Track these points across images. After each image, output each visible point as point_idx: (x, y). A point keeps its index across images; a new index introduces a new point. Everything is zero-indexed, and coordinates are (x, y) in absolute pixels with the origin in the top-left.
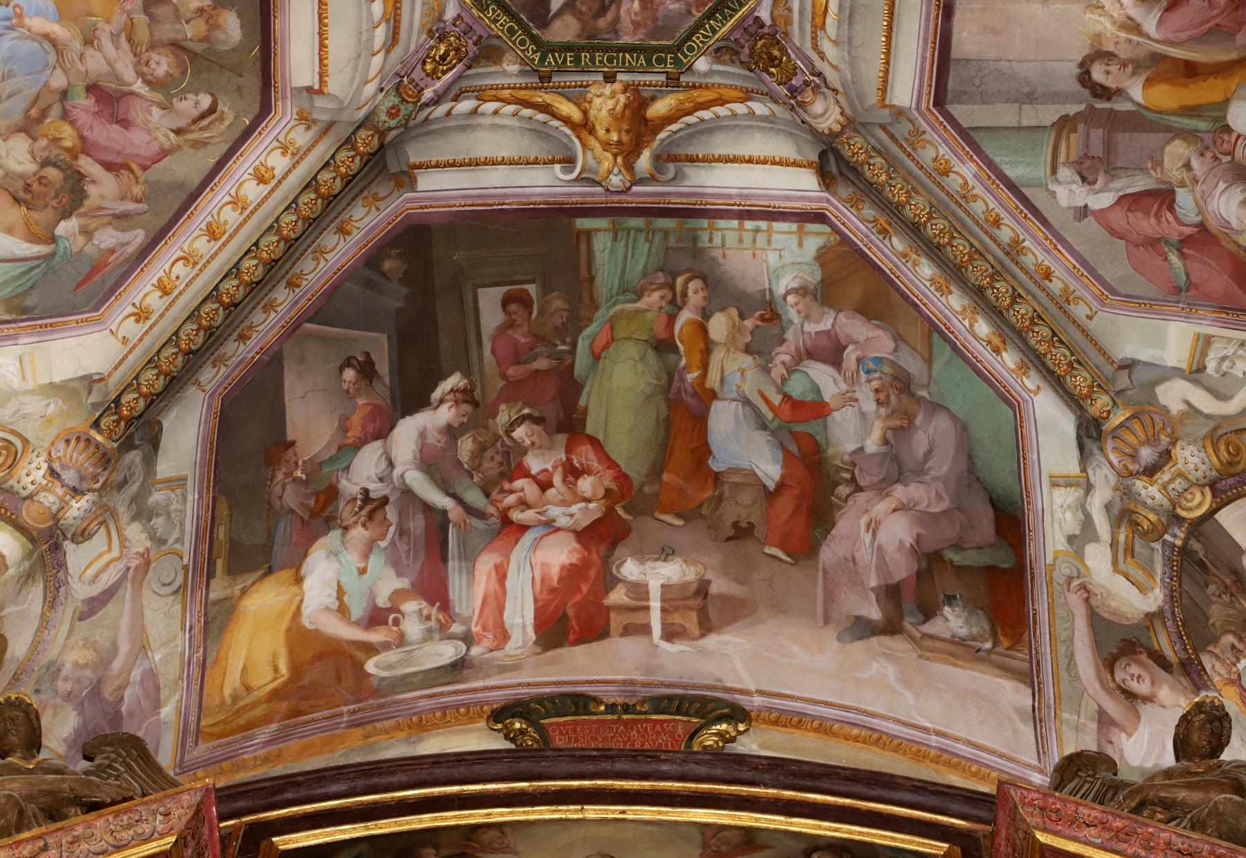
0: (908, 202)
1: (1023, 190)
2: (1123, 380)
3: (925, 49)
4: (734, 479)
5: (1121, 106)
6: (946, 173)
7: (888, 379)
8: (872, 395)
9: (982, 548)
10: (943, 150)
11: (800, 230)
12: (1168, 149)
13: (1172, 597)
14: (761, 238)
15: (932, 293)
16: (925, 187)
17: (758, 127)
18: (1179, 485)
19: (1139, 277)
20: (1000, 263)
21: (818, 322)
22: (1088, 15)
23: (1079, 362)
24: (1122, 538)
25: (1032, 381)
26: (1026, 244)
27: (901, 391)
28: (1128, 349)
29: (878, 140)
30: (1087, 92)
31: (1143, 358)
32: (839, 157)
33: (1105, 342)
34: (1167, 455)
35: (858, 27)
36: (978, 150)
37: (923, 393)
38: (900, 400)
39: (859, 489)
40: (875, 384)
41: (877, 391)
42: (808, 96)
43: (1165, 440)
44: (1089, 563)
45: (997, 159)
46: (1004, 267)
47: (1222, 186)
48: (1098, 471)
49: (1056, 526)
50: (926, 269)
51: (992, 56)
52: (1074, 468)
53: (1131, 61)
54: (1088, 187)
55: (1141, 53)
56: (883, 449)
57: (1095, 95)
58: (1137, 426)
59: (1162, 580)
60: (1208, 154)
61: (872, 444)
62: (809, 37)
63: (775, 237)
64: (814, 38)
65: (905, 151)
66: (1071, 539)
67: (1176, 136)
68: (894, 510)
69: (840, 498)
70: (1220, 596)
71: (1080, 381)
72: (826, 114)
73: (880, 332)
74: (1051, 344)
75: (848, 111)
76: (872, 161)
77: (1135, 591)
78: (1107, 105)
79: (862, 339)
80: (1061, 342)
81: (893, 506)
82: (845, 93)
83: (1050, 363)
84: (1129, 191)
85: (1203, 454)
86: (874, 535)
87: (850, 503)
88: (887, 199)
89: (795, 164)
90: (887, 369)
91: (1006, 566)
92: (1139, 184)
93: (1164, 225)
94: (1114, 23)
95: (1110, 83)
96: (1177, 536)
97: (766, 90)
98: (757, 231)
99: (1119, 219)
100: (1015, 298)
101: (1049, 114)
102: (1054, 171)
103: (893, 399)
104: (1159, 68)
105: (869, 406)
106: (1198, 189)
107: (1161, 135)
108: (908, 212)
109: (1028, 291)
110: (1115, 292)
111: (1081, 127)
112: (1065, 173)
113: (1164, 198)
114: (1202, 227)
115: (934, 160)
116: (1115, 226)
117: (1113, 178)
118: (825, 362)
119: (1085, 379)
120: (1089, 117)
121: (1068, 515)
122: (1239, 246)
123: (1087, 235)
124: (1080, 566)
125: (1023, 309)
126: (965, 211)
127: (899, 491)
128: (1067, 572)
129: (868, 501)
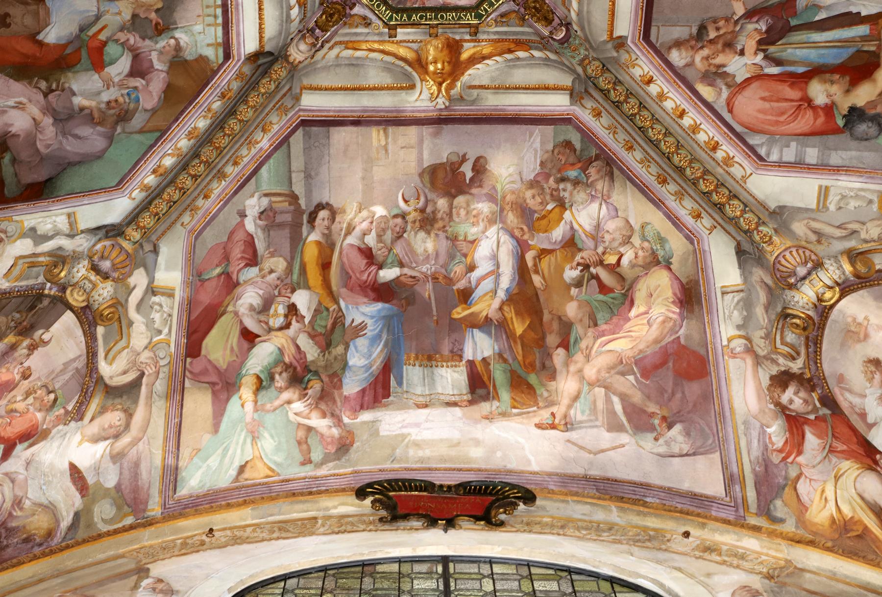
0: (249, 107)
1: (254, 178)
2: (148, 247)
3: (334, 111)
4: (42, 12)
5: (305, 229)
6: (264, 130)
7: (126, 108)
8: (113, 98)
9: (16, 175)
10: (276, 128)
11: (218, 44)
12: (281, 259)
13: (5, 293)
14: (211, 20)
15: (188, 127)
16: (257, 117)
17: (282, 13)
18: (88, 286)
19: (206, 252)
20: (215, 167)
21: (159, 60)
22: (355, 205)
23: (158, 219)
24: (41, 259)
25: (138, 195)
26: (223, 182)
27: (119, 115)
28: (165, 250)
29: (284, 86)
30: (312, 209)
31: (159, 259)
32: (272, 63)
33: (169, 234)
34: (106, 277)
35: (346, 70)
36: (276, 148)
37: (119, 129)
38: (112, 115)
39: (46, 95)
40: (121, 100)
41: (116, 101)
42: (310, 40)
43: (116, 275)
44: (18, 242)
45: (271, 161)
46: (212, 169)
47: (261, 292)
48: (84, 240)
49: (40, 220)
50: (202, 124)
51: (331, 151)
52: (82, 226)
53: (330, 232)
54: (257, 215)
55: (335, 236)
56: (76, 108)
57: (311, 214)
58: (121, 258)
59: (15, 286)
60: (279, 282)
61: (78, 101)
62: (342, 39)
63: (213, 29)
64: (340, 43)
65: (277, 103)
66: (33, 230)
67: (288, 263)
68: (34, 119)
69: (37, 83)
70: (12, 320)
71: (147, 220)
72: (298, 52)
73: (156, 100)
74: (169, 201)
75: (301, 66)
76: (272, 82)
77: (5, 271)
78: (305, 221)
79: (151, 88)
80: (170, 207)
81: (36, 117)
82: (310, 64)
83: (156, 202)
84: (256, 241)
85: (108, 298)
86: (13, 107)
87: (35, 90)
88: (249, 94)
89: (261, 38)
90: (132, 106)
91: (6, 192)
92: (260, 245)
93: (237, 263)
94: (351, 220)
95: (318, 221)
96: (50, 290)
97: (308, 15)
98: (215, 17)
99: (240, 236)
100: (195, 177)
101: (299, 189)
102: (266, 195)
103: (112, 112)
104: (327, 247)
105: (105, 97)
106: (259, 279)
107: (289, 254)
108: (242, 108)
109: (199, 185)
110: (196, 238)
111: (292, 208)
112: (265, 201)
113: (253, 260)
114: (237, 284)
115: (271, 122)
116: (235, 234)
117: (263, 230)
118: (132, 66)
119: (149, 224)
120: (298, 212)
121: (49, 226)
122: (227, 306)
123: (229, 218)
124: (15, 237)
125: (189, 182)
126: (243, 143)
127: (48, 121)
128: (9, 229)
129: (38, 102)
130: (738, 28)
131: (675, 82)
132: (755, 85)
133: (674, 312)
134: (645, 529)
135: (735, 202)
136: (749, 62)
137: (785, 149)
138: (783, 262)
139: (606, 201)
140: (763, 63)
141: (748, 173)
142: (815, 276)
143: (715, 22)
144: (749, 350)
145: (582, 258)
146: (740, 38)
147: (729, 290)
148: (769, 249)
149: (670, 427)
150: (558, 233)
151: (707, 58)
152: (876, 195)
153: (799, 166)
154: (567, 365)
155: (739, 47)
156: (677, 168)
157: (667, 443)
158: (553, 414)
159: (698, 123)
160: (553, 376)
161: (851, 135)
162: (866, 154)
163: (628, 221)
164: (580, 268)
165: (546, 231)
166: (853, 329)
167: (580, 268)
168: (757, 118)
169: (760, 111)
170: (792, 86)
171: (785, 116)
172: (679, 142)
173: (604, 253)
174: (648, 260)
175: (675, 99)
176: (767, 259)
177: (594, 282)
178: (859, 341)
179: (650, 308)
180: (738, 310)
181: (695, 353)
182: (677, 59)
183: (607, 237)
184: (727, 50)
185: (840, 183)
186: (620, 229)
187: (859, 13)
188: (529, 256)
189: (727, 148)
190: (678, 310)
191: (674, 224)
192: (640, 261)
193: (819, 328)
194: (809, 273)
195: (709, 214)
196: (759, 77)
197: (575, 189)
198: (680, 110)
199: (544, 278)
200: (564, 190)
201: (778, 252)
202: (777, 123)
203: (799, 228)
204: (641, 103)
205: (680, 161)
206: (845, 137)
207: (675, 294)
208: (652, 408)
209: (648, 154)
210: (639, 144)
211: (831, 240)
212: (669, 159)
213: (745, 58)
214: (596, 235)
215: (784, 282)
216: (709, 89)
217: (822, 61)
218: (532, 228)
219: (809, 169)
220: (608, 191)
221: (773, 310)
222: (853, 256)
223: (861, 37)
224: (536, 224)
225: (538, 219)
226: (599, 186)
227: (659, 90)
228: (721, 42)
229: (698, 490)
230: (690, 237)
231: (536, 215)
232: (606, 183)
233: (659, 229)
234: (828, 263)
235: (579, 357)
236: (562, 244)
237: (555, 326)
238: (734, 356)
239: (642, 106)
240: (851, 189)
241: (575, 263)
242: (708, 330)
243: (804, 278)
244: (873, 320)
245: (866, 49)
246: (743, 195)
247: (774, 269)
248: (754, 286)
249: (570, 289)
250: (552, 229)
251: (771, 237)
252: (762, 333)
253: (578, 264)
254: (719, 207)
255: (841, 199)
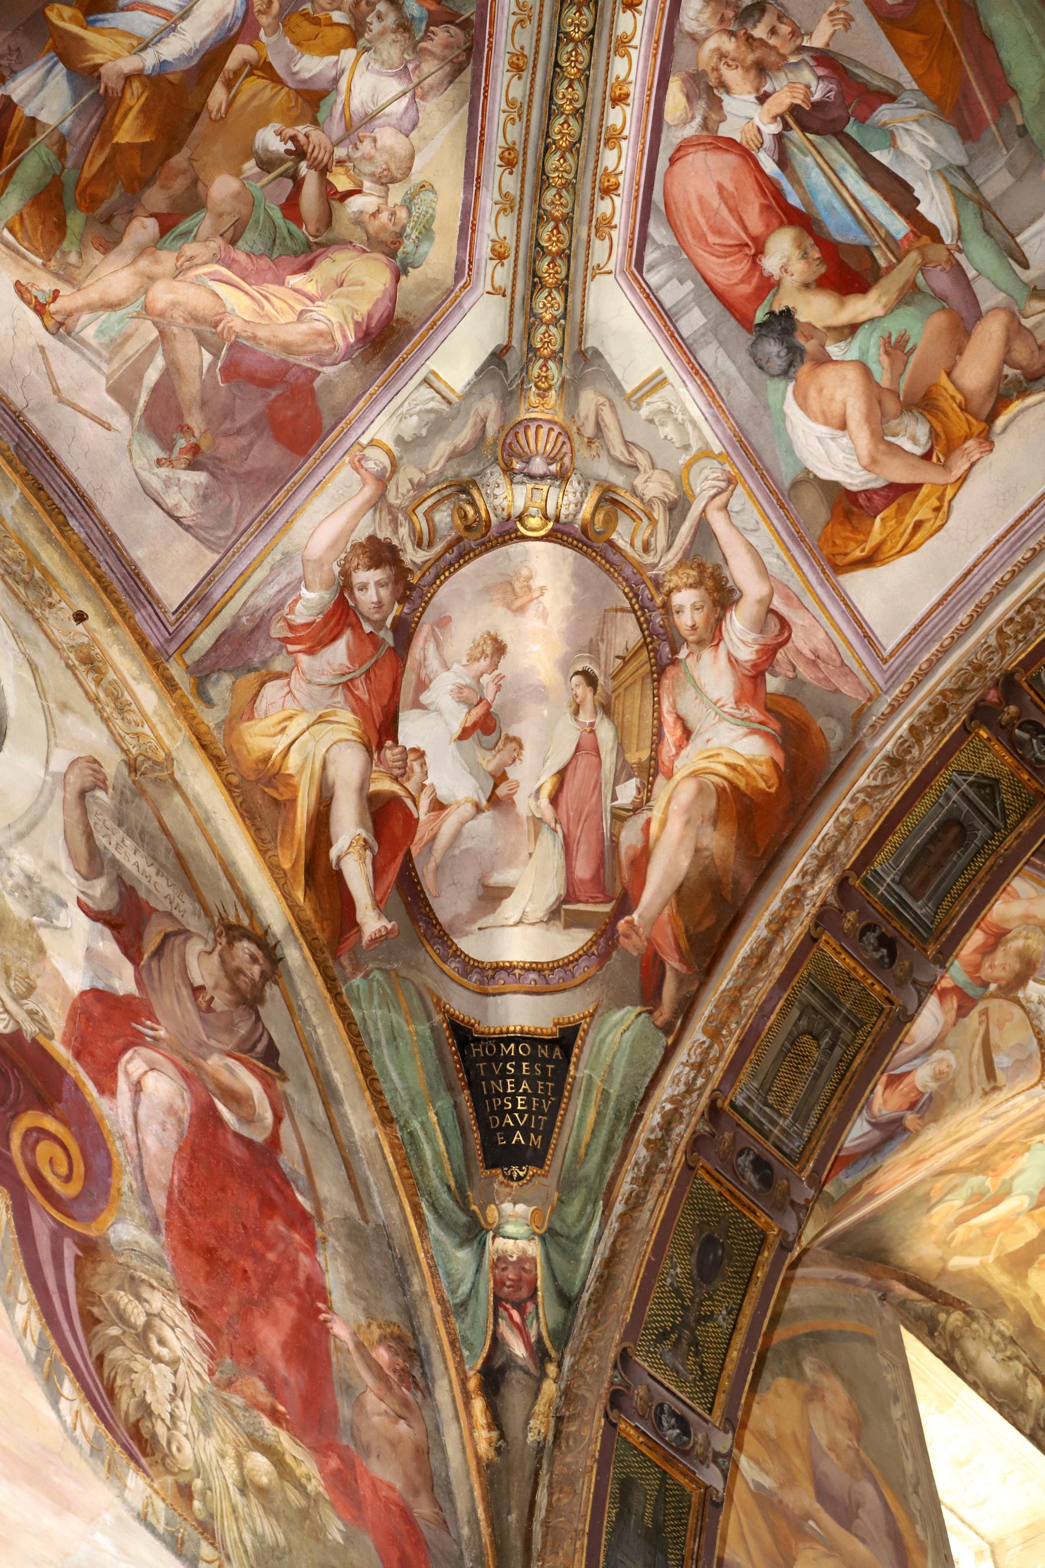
130: (792, 59)
131: (657, 42)
132: (731, 159)
133: (344, 337)
134: (34, 559)
135: (559, 298)
136: (757, 122)
137: (675, 282)
138: (531, 433)
139: (414, 97)
140: (768, 142)
141: (611, 266)
142: (545, 488)
143: (780, 18)
144: (383, 480)
145: (307, 136)
146: (782, 76)
147: (437, 384)
148: (534, 399)
149: (192, 466)
150: (311, 66)
151: (722, 56)
152: (700, 444)
153: (665, 318)
154: (142, 251)
155: (768, 87)
156: (543, 173)
157: (167, 483)
158: (56, 294)
159: (625, 133)
160: (109, 244)
161: (754, 344)
162: (742, 384)
163: (412, 157)
164: (290, 146)
165: (298, 44)
166: (517, 585)
167: (290, 146)
168: (689, 205)
169: (701, 199)
170: (766, 209)
171: (718, 241)
172: (579, 141)
173: (340, 162)
174: (384, 236)
175: (631, 69)
176: (518, 408)
177: (289, 184)
178: (508, 606)
179: (322, 299)
180: (421, 420)
181: (316, 413)
182: (691, 14)
183: (366, 147)
184: (752, 74)
185: (682, 390)
186: (393, 155)
187: (918, 201)
188: (241, 52)
189: (618, 209)
190: (352, 340)
191: (463, 229)
192: (373, 226)
193: (483, 544)
194: (543, 477)
195: (515, 273)
196: (746, 155)
197: (394, 32)
198: (625, 90)
199: (230, 104)
200: (380, 17)
201: (539, 416)
202: (702, 238)
203: (589, 400)
204: (592, 32)
205: (556, 169)
206: (745, 338)
207: (370, 316)
208: (195, 420)
209: (530, 107)
210: (533, 80)
211: (603, 453)
212: (547, 148)
213: (759, 108)
214: (357, 127)
215: (508, 454)
216: (683, 100)
217: (824, 215)
218: (284, 19)
219: (672, 336)
220: (432, 88)
221: (459, 465)
222: (610, 501)
223: (888, 233)
224: (296, 19)
225: (305, 15)
226: (429, 66)
227: (629, 32)
228: (758, 54)
229: (147, 572)
230: (464, 268)
231: (308, 6)
232: (440, 74)
233: (438, 214)
234: (574, 486)
235: (168, 259)
236: (302, 87)
237: (179, 184)
238: (358, 466)
239: (590, 38)
240: (685, 411)
241: (290, 132)
242: (361, 403)
243: (532, 477)
244: (547, 600)
245: (877, 254)
246: (575, 296)
247: (514, 429)
248: (468, 414)
249: (247, 159)
250: (310, 50)
251: (550, 387)
252: (417, 476)
253: (294, 139)
254: (535, 283)
255: (663, 411)
